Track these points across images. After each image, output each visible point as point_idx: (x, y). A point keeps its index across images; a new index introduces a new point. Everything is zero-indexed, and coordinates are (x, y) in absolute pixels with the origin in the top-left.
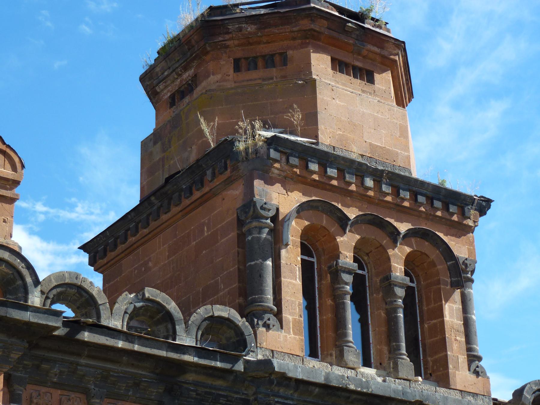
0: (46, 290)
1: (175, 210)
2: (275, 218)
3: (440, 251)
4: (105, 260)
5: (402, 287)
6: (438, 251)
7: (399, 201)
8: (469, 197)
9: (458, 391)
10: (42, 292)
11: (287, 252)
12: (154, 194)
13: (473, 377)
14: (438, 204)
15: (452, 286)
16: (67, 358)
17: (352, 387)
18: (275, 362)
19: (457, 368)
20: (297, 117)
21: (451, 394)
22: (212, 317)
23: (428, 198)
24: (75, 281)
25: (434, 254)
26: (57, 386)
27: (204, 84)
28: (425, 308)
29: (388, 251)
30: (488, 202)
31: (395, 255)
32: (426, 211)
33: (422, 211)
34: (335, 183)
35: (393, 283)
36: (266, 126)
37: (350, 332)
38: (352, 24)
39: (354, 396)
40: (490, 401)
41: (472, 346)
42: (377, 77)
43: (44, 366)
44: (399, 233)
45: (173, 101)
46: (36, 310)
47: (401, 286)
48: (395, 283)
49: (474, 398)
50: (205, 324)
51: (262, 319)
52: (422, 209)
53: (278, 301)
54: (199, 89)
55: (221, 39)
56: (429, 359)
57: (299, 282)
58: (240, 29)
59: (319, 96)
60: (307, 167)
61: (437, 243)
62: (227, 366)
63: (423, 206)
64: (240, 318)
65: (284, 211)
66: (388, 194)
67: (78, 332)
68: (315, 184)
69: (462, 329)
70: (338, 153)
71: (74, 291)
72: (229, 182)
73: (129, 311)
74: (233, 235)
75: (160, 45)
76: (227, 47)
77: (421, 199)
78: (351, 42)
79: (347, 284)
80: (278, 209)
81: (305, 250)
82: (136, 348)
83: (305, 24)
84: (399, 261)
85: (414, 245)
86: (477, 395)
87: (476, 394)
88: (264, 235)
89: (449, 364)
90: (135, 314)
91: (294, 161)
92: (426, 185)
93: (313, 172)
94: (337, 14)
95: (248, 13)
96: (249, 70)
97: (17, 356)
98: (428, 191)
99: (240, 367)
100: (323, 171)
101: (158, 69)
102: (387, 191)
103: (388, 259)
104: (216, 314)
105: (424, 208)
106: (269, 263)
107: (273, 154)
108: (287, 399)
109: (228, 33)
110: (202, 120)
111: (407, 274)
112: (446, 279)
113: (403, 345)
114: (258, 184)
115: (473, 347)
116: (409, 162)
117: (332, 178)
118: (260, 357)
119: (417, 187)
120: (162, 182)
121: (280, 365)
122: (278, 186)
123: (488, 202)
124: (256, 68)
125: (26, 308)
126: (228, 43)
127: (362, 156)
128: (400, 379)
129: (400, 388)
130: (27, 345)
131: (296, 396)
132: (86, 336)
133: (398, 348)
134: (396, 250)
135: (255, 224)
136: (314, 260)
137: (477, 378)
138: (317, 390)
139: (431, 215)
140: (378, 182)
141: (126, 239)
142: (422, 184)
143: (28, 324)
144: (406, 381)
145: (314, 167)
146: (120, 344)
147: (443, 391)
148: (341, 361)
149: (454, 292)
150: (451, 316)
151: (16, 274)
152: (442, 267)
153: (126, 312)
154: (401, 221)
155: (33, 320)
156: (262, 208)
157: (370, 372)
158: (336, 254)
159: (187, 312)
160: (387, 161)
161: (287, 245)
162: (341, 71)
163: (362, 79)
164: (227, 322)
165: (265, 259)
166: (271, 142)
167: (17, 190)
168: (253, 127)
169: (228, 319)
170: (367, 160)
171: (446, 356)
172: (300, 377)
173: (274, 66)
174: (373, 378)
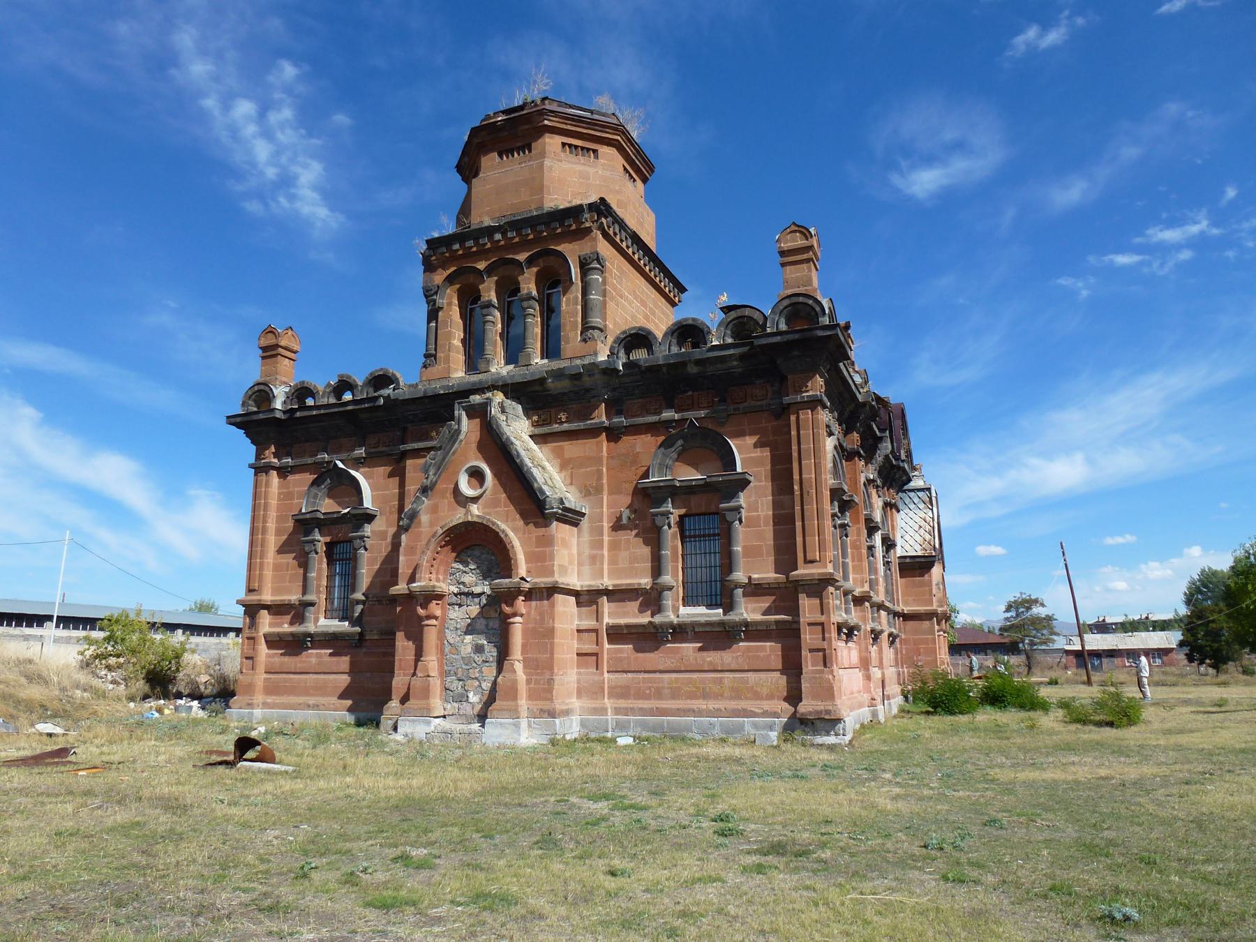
17: (442, 392)
26: (307, 441)
34: (474, 249)
52: (545, 234)
62: (371, 405)
67: (294, 414)
93: (458, 250)
134: (525, 275)
138: (426, 400)
146: (314, 413)
150: (567, 305)
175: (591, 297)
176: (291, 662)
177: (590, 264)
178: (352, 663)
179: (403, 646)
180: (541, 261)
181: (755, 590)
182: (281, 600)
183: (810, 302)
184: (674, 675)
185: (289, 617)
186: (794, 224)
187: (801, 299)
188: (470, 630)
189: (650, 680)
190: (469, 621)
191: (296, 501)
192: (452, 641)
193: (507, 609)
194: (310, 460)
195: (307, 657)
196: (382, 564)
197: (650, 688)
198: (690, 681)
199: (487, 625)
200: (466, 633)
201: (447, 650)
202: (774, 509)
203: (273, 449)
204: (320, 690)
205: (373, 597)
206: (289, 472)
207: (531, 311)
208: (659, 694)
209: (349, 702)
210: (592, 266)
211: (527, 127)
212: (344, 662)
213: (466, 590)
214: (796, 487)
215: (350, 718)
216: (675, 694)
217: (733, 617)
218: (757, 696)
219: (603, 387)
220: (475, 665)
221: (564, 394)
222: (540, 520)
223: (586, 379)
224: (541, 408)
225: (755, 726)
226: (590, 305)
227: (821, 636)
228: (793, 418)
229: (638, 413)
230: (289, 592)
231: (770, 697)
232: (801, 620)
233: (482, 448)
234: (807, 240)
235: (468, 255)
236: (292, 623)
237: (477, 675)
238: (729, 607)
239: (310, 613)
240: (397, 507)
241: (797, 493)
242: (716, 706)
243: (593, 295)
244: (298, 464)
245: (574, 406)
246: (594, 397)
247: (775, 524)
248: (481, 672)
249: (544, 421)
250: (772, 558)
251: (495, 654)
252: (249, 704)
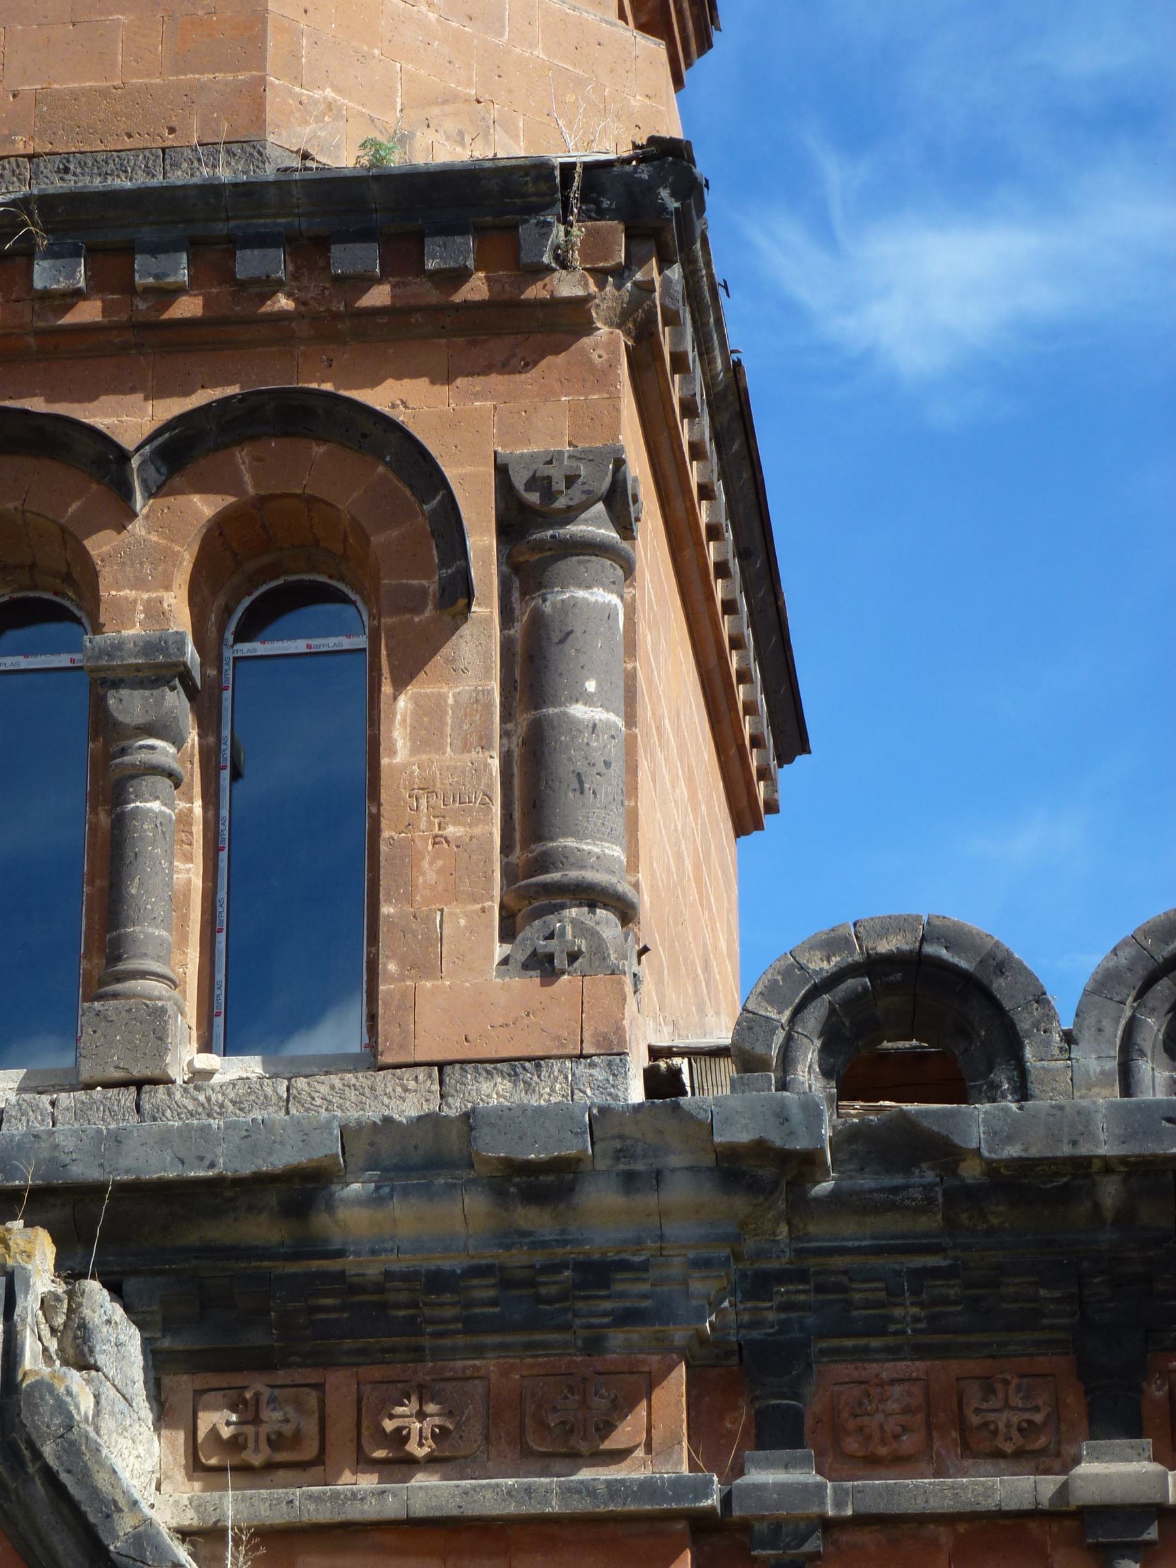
3: (386, 464)
6: (381, 469)
7: (142, 306)
8: (527, 175)
9: (421, 1072)
13: (533, 981)
21: (379, 1091)
29: (85, 542)
32: (303, 308)
33: (283, 315)
35: (102, 675)
40: (614, 1075)
41: (551, 844)
44: (124, 456)
48: (111, 675)
49: (515, 1083)
52: (284, 302)
61: (364, 436)
63: (286, 288)
66: (76, 295)
84: (147, 568)
85: (247, 478)
86: (538, 1066)
87: (529, 1060)
89: (381, 960)
92: (273, 191)
98: (299, 216)
102: (62, 285)
105: (289, 295)
112: (415, 582)
115: (558, 847)
116: (259, 106)
119: (228, 219)
128: (89, 1086)
134: (138, 528)
137: (542, 985)
139: (336, 316)
144: (116, 1090)
147: (332, 1087)
149: (457, 628)
160: (128, 143)
170: (13, 171)
175: (579, 711)
177: (570, 514)
180: (242, 457)
207: (163, 751)
210: (579, 529)
219: (702, 1264)
221: (437, 1281)
224: (263, 1361)
226: (566, 763)
229: (908, 1443)
243: (588, 700)
245: (490, 1365)
246: (628, 1318)
249: (277, 1441)
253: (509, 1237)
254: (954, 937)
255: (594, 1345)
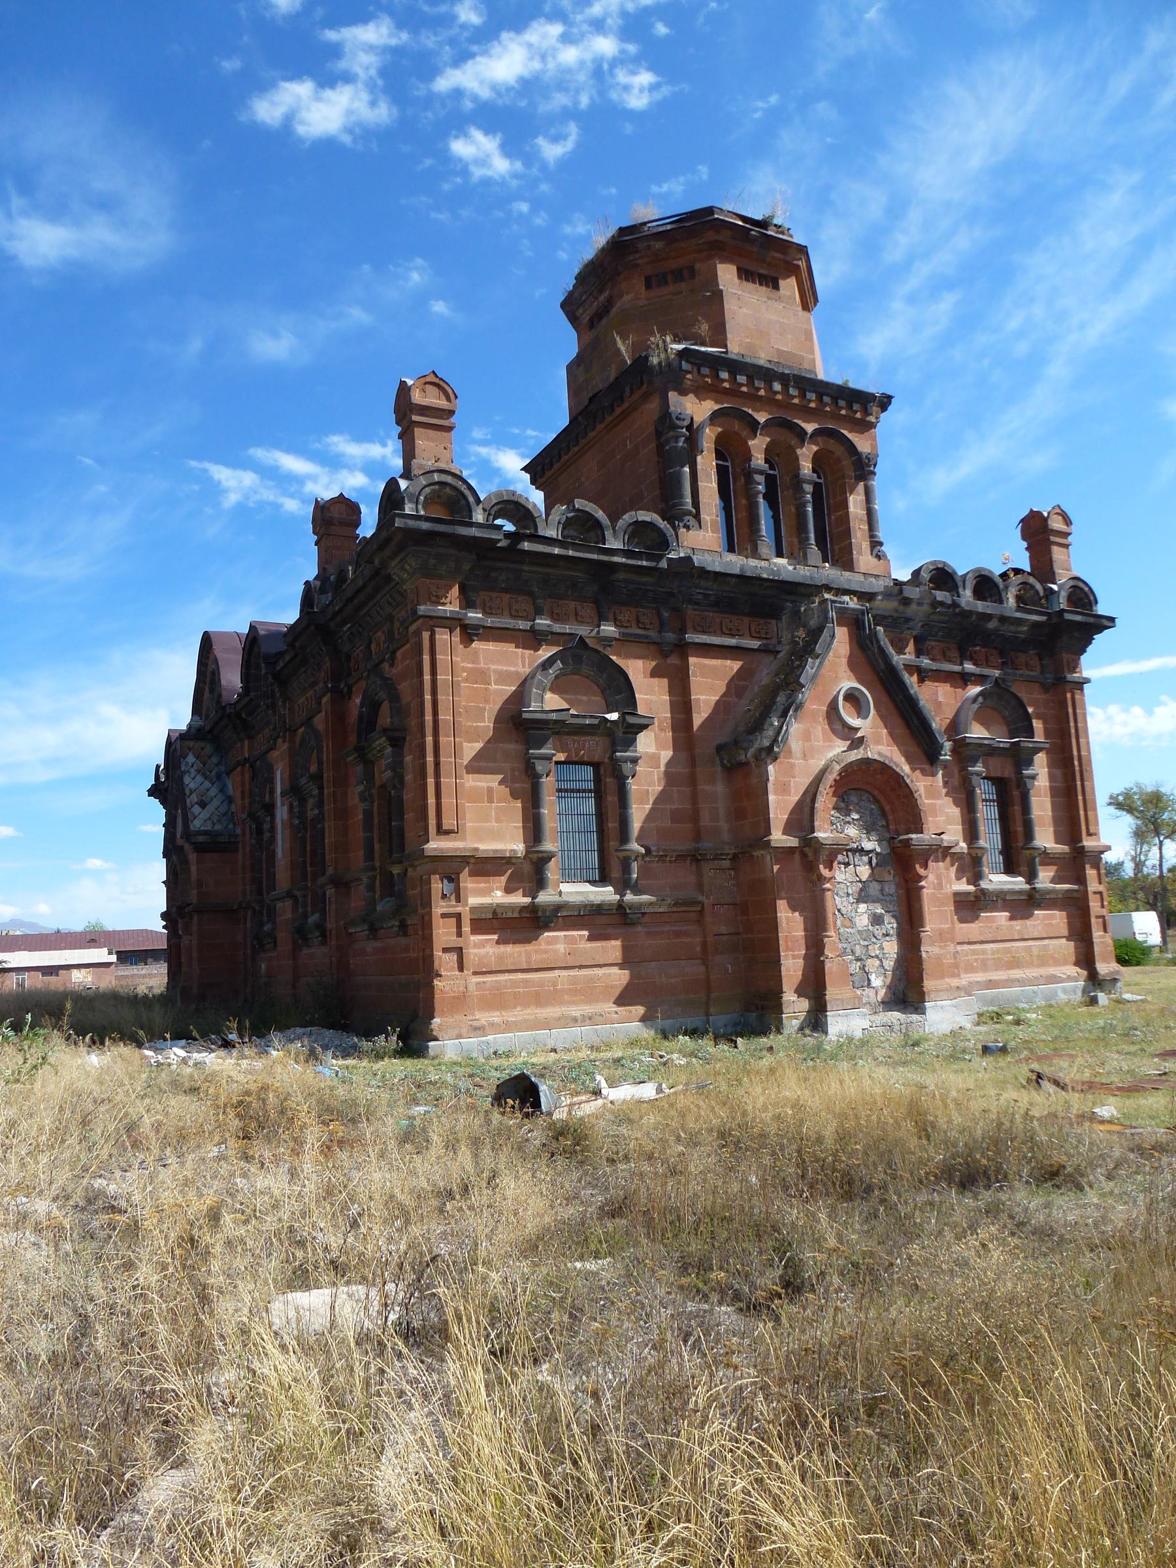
0: (488, 508)
1: (600, 427)
2: (690, 427)
4: (544, 479)
5: (810, 484)
10: (484, 510)
11: (703, 458)
12: (580, 413)
13: (875, 560)
14: (842, 403)
15: (856, 479)
16: (512, 566)
17: (765, 576)
18: (695, 558)
19: (860, 553)
20: (704, 328)
22: (637, 522)
23: (832, 398)
24: (513, 498)
25: (839, 450)
26: (505, 590)
27: (619, 304)
28: (832, 501)
30: (890, 398)
31: (803, 454)
34: (744, 389)
36: (675, 341)
37: (763, 527)
38: (755, 232)
39: (767, 584)
42: (782, 283)
43: (493, 574)
44: (806, 433)
45: (592, 324)
46: (479, 525)
47: (809, 482)
50: (631, 528)
51: (682, 521)
52: (828, 409)
53: (696, 503)
54: (614, 310)
55: (631, 258)
56: (836, 547)
57: (715, 485)
58: (649, 247)
59: (726, 306)
60: (718, 376)
62: (653, 564)
64: (661, 521)
65: (698, 419)
66: (795, 397)
68: (726, 392)
69: (865, 518)
70: (748, 360)
71: (512, 506)
72: (646, 397)
73: (562, 522)
74: (653, 446)
75: (576, 271)
76: (638, 265)
77: (826, 399)
78: (755, 250)
79: (759, 484)
80: (692, 419)
81: (719, 455)
82: (571, 553)
83: (711, 236)
88: (681, 444)
90: (567, 524)
91: (705, 371)
93: (724, 381)
94: (740, 223)
95: (655, 231)
96: (659, 286)
97: (468, 567)
99: (664, 564)
100: (733, 379)
101: (576, 295)
103: (797, 459)
104: (640, 519)
106: (687, 469)
107: (685, 365)
108: (707, 589)
109: (637, 252)
110: (618, 339)
111: (814, 471)
113: (812, 536)
114: (672, 396)
117: (741, 385)
118: (682, 555)
120: (586, 403)
121: (699, 560)
122: (691, 396)
123: (890, 398)
124: (666, 283)
125: (471, 524)
126: (638, 261)
127: (770, 361)
129: (808, 574)
130: (475, 557)
131: (715, 586)
132: (526, 546)
133: (808, 539)
134: (804, 449)
135: (671, 434)
136: (729, 464)
140: (785, 386)
141: (560, 458)
142: (827, 385)
143: (474, 538)
145: (724, 375)
146: (556, 551)
148: (755, 554)
150: (855, 507)
151: (460, 496)
152: (847, 463)
153: (559, 523)
154: (808, 422)
155: (478, 535)
156: (679, 419)
157: (782, 561)
158: (748, 457)
159: (614, 518)
161: (702, 451)
162: (747, 280)
163: (767, 286)
164: (650, 525)
165: (683, 466)
166: (682, 354)
167: (453, 420)
168: (664, 342)
169: (651, 523)
171: (851, 543)
172: (718, 569)
173: (682, 279)
174: (784, 567)
176: (515, 952)
178: (625, 949)
179: (787, 918)
181: (1048, 858)
182: (496, 851)
183: (1086, 589)
184: (992, 945)
185: (503, 879)
186: (1059, 506)
187: (1081, 585)
188: (862, 897)
189: (974, 952)
190: (860, 885)
191: (494, 687)
192: (844, 911)
193: (921, 871)
194: (523, 625)
195: (548, 943)
196: (654, 803)
197: (976, 960)
198: (1007, 951)
199: (882, 890)
200: (859, 900)
201: (839, 922)
202: (1050, 781)
203: (455, 591)
204: (587, 993)
205: (658, 851)
206: (477, 635)
208: (984, 967)
209: (640, 1010)
211: (778, 255)
212: (613, 948)
213: (855, 846)
214: (1076, 763)
215: (647, 1034)
216: (999, 965)
217: (544, 897)
218: (1057, 963)
220: (875, 940)
222: (927, 767)
223: (914, 607)
225: (1064, 991)
227: (1099, 904)
228: (1069, 695)
230: (497, 836)
231: (1065, 963)
232: (1089, 889)
233: (852, 665)
234: (1068, 525)
235: (753, 398)
236: (508, 890)
237: (878, 952)
238: (1031, 877)
239: (552, 871)
240: (669, 721)
241: (1077, 768)
242: (1034, 974)
244: (499, 625)
246: (909, 629)
247: (1052, 796)
248: (881, 948)
250: (1052, 829)
251: (895, 925)
252: (476, 1029)
253: (896, 611)
254: (949, 566)
255: (902, 632)
